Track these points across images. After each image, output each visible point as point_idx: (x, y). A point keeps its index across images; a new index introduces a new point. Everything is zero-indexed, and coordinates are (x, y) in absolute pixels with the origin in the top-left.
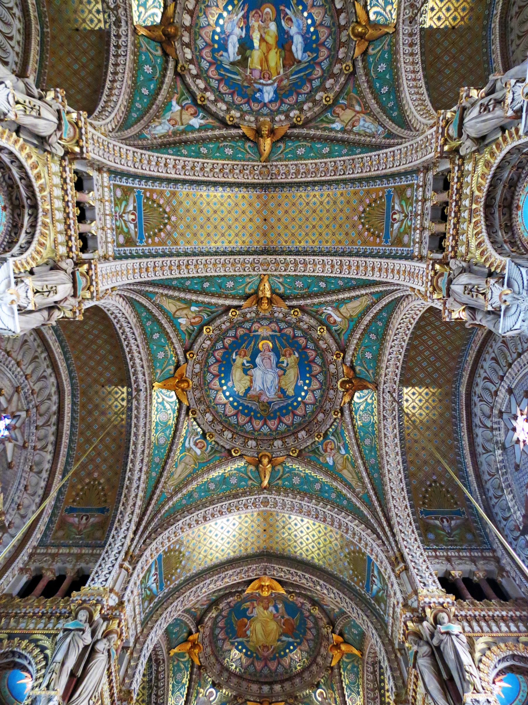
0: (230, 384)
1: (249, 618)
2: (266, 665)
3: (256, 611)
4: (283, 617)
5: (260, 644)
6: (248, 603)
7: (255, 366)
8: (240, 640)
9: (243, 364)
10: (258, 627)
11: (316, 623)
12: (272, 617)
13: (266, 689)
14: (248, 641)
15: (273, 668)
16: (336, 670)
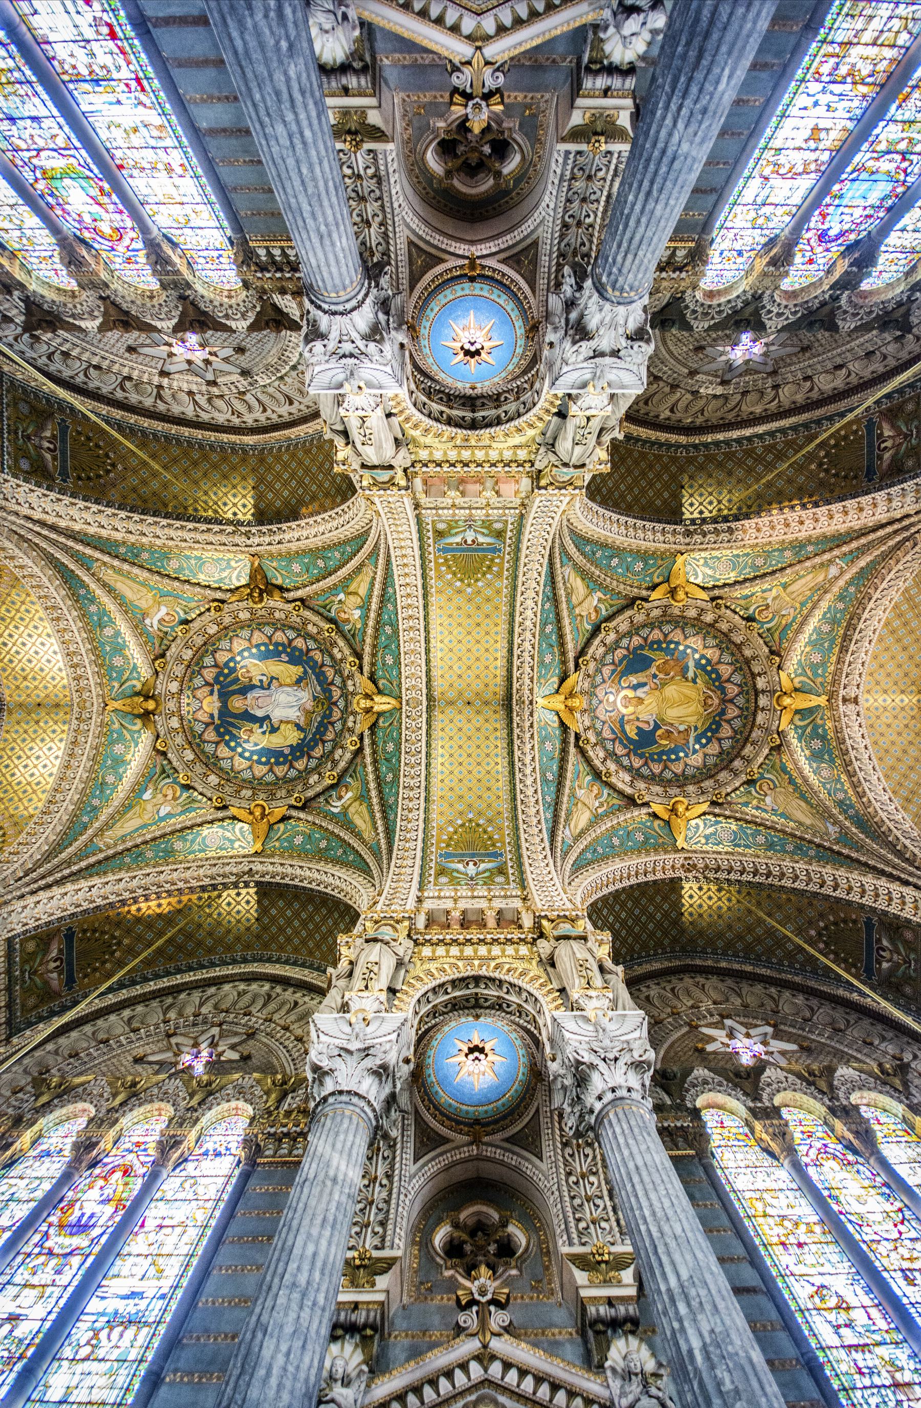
0: (287, 751)
1: (657, 727)
2: (731, 701)
3: (644, 717)
4: (655, 676)
5: (701, 710)
6: (627, 728)
7: (268, 717)
8: (691, 740)
9: (264, 733)
10: (672, 714)
11: (651, 625)
12: (657, 693)
13: (763, 701)
14: (696, 728)
15: (737, 690)
16: (716, 592)
